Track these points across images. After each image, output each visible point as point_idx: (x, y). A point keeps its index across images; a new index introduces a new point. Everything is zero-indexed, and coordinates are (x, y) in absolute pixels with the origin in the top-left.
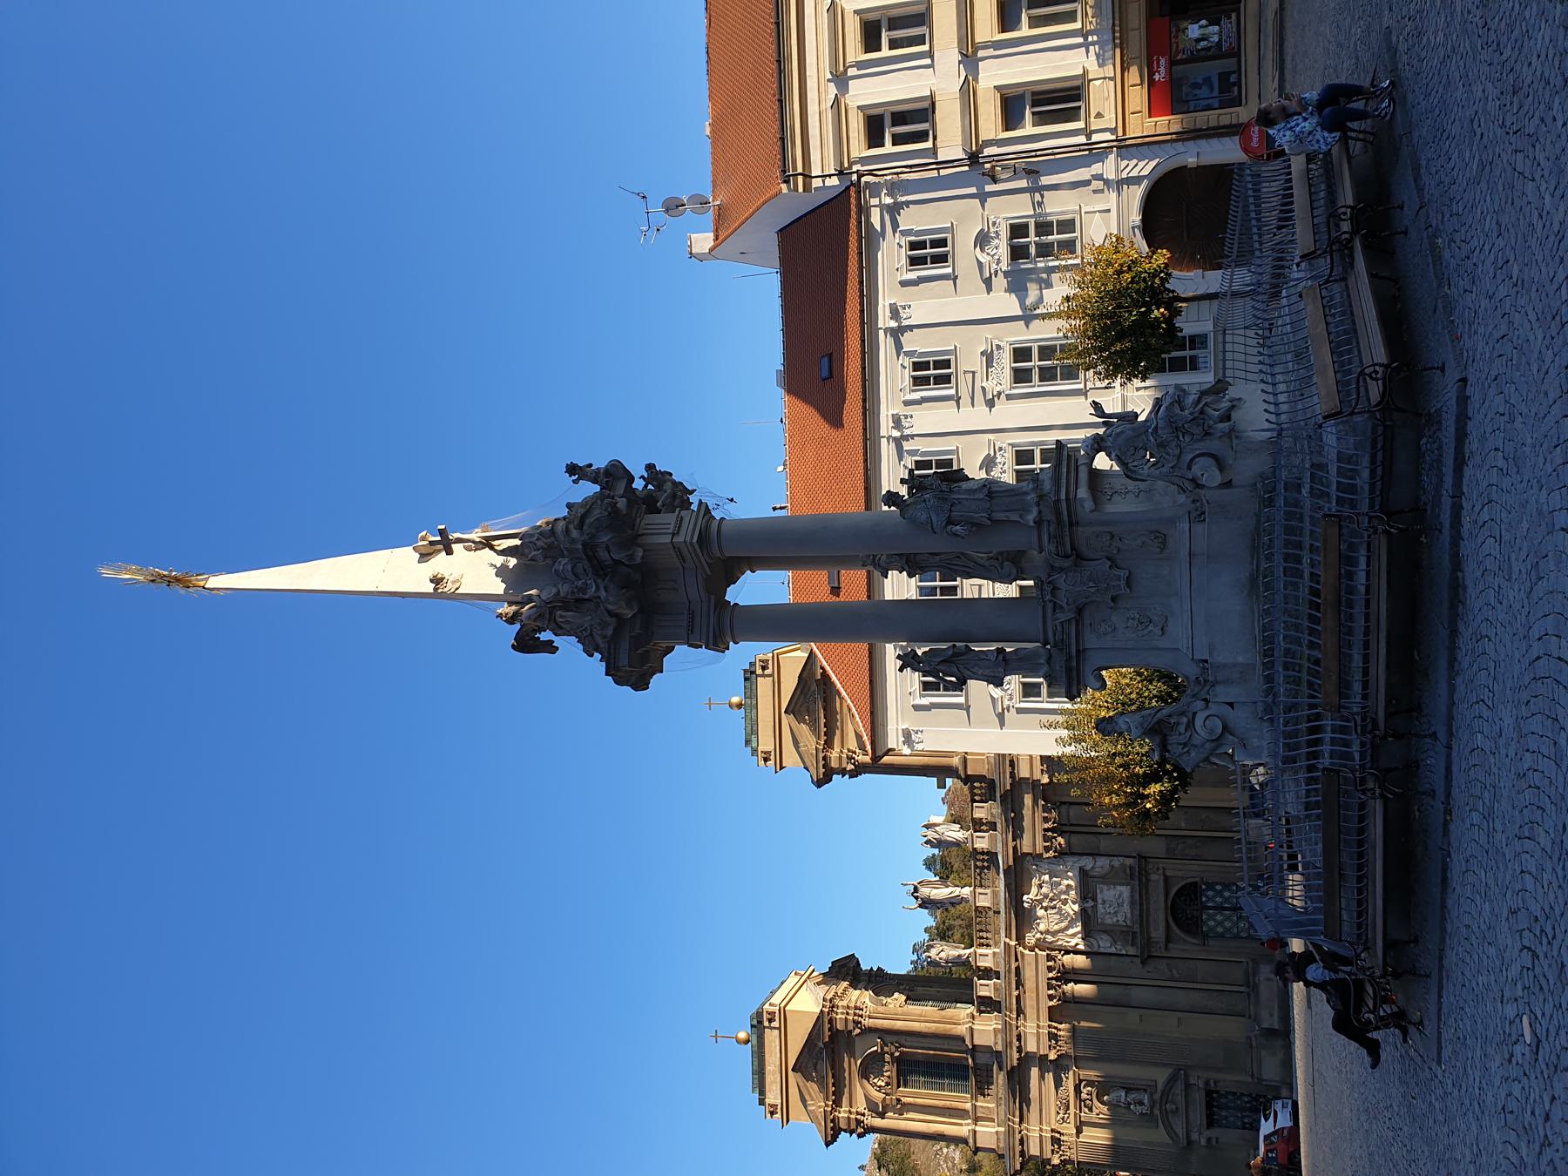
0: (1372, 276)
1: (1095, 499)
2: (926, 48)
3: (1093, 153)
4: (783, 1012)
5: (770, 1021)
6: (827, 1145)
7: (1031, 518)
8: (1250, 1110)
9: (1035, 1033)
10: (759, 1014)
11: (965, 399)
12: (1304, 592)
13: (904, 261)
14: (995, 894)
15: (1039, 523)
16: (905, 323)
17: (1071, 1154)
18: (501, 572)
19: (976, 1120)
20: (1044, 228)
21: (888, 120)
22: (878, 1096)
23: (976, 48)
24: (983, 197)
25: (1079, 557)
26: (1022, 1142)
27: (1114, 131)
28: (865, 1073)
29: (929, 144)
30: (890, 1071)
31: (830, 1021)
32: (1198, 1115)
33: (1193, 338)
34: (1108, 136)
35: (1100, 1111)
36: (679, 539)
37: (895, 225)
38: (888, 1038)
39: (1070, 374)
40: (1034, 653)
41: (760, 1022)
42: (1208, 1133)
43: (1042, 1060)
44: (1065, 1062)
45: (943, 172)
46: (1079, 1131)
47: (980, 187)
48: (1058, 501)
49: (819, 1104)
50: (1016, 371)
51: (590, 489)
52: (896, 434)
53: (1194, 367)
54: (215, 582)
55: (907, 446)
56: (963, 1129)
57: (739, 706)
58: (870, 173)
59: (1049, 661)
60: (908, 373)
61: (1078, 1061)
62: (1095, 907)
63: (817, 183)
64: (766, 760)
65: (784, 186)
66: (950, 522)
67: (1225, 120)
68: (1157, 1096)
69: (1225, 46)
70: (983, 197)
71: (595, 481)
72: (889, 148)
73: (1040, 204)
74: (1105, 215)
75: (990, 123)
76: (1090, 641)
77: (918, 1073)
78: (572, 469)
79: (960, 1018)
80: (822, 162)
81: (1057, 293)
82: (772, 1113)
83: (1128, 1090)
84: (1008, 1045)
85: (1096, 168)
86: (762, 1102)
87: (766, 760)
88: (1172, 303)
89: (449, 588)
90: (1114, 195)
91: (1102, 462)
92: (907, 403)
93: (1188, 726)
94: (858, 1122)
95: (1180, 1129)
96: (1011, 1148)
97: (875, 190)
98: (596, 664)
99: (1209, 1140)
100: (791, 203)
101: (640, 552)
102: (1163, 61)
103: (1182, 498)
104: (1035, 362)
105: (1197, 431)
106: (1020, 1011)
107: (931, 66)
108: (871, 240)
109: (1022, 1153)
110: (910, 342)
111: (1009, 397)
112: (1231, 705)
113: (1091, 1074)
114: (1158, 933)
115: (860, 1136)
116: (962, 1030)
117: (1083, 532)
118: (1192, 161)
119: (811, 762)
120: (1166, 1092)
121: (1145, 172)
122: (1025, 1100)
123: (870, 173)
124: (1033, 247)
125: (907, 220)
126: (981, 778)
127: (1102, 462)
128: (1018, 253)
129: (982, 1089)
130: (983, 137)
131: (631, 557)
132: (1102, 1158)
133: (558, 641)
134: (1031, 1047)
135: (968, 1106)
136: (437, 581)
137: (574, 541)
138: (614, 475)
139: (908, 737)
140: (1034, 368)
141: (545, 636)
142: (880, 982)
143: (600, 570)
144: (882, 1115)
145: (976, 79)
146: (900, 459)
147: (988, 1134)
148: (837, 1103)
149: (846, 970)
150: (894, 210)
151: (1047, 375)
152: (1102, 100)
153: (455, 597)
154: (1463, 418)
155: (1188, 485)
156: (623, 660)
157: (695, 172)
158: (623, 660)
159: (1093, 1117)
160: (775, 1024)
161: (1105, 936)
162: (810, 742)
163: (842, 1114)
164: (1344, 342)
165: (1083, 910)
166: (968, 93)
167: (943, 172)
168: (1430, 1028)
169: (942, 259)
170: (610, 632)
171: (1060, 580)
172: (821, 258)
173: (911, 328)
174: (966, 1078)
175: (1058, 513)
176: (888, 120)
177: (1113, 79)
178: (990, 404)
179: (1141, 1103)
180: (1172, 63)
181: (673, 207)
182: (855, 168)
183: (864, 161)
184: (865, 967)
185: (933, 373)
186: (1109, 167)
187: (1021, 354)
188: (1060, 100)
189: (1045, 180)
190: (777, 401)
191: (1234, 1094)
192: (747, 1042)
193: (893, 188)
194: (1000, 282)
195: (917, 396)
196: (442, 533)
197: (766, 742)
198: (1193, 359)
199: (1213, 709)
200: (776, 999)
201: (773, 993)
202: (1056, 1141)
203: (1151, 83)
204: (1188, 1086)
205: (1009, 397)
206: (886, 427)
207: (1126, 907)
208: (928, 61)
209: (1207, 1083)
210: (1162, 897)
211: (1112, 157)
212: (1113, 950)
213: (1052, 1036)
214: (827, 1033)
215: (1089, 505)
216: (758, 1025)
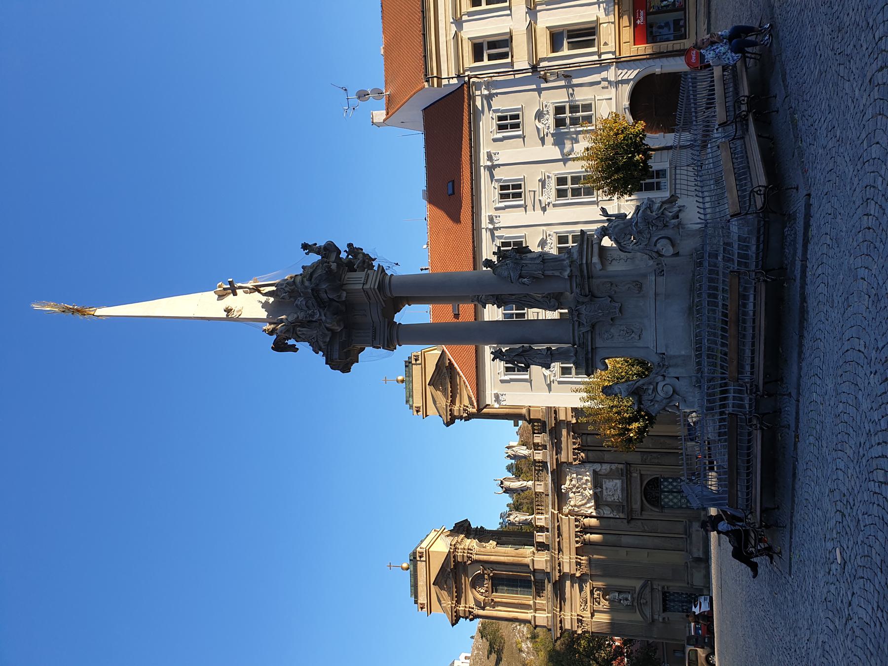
0: (758, 136)
1: (602, 263)
3: (603, 66)
4: (428, 552)
5: (420, 557)
6: (453, 625)
7: (566, 274)
8: (686, 602)
9: (568, 562)
10: (414, 553)
11: (530, 207)
12: (719, 315)
13: (495, 127)
14: (546, 485)
15: (570, 277)
16: (496, 163)
17: (588, 628)
18: (265, 305)
19: (536, 610)
20: (574, 108)
21: (485, 46)
22: (481, 598)
23: (536, 5)
24: (539, 91)
25: (593, 296)
27: (614, 53)
28: (474, 585)
29: (509, 60)
30: (487, 584)
31: (454, 557)
32: (658, 606)
33: (658, 172)
34: (611, 56)
35: (604, 604)
36: (367, 287)
37: (490, 106)
38: (487, 566)
39: (589, 192)
40: (567, 351)
41: (415, 558)
42: (664, 615)
44: (585, 578)
45: (517, 76)
46: (593, 615)
47: (538, 85)
48: (581, 264)
49: (448, 603)
50: (558, 191)
51: (315, 258)
52: (491, 226)
53: (659, 188)
54: (100, 312)
55: (497, 233)
56: (528, 615)
57: (402, 381)
58: (476, 76)
59: (576, 354)
60: (497, 192)
61: (592, 577)
62: (601, 492)
63: (445, 82)
64: (418, 411)
65: (426, 84)
66: (521, 276)
67: (677, 47)
68: (636, 596)
69: (677, 4)
70: (539, 91)
71: (318, 253)
72: (486, 62)
73: (572, 95)
74: (609, 101)
75: (544, 48)
76: (599, 343)
77: (503, 585)
78: (305, 246)
79: (526, 554)
80: (448, 70)
81: (581, 146)
82: (422, 608)
83: (620, 592)
84: (553, 569)
85: (604, 74)
86: (416, 602)
87: (418, 411)
88: (647, 152)
89: (235, 314)
90: (614, 90)
91: (607, 242)
92: (497, 209)
93: (653, 390)
94: (470, 612)
95: (648, 613)
96: (555, 625)
97: (478, 86)
98: (320, 358)
99: (664, 619)
100: (430, 93)
101: (344, 294)
102: (642, 13)
103: (651, 262)
104: (569, 186)
105: (660, 224)
106: (560, 550)
107: (510, 15)
108: (476, 115)
109: (561, 628)
110: (499, 174)
111: (554, 206)
112: (678, 378)
113: (599, 584)
114: (637, 506)
115: (471, 620)
116: (527, 561)
117: (595, 282)
118: (658, 71)
119: (443, 412)
120: (641, 593)
121: (632, 77)
122: (563, 599)
123: (476, 76)
124: (568, 120)
125: (496, 103)
126: (538, 420)
127: (607, 242)
128: (559, 123)
129: (539, 592)
130: (540, 56)
131: (340, 297)
132: (605, 630)
133: (298, 345)
134: (566, 569)
135: (531, 603)
136: (228, 311)
137: (306, 288)
138: (329, 249)
139: (497, 398)
140: (569, 189)
141: (291, 342)
142: (482, 535)
143: (322, 304)
144: (483, 609)
145: (536, 23)
146: (493, 241)
147: (542, 618)
148: (458, 602)
149: (463, 528)
150: (489, 98)
151: (576, 193)
152: (607, 34)
153: (238, 320)
154: (808, 216)
155: (654, 255)
156: (336, 355)
157: (374, 75)
158: (336, 355)
159: (600, 607)
160: (423, 559)
161: (607, 508)
162: (443, 401)
163: (461, 608)
164: (742, 174)
165: (595, 494)
166: (531, 30)
167: (517, 76)
168: (785, 555)
169: (517, 126)
170: (328, 340)
171: (582, 309)
172: (448, 125)
173: (499, 166)
174: (530, 587)
175: (581, 271)
176: (485, 46)
177: (613, 23)
178: (544, 209)
179: (627, 599)
180: (647, 14)
181: (362, 95)
182: (467, 74)
183: (472, 69)
184: (473, 526)
185: (511, 192)
186: (611, 74)
187: (561, 181)
188: (584, 35)
189: (575, 81)
190: (423, 207)
191: (678, 593)
192: (407, 569)
193: (489, 85)
194: (549, 140)
195: (502, 205)
196: (230, 283)
197: (418, 402)
198: (658, 183)
199: (668, 380)
200: (424, 545)
201: (422, 541)
202: (580, 621)
203: (635, 26)
204: (652, 589)
205: (554, 206)
206: (485, 223)
207: (619, 492)
208: (508, 12)
209: (663, 588)
210: (639, 487)
211: (613, 68)
212: (611, 515)
213: (578, 564)
214: (452, 564)
215: (599, 266)
216: (414, 559)
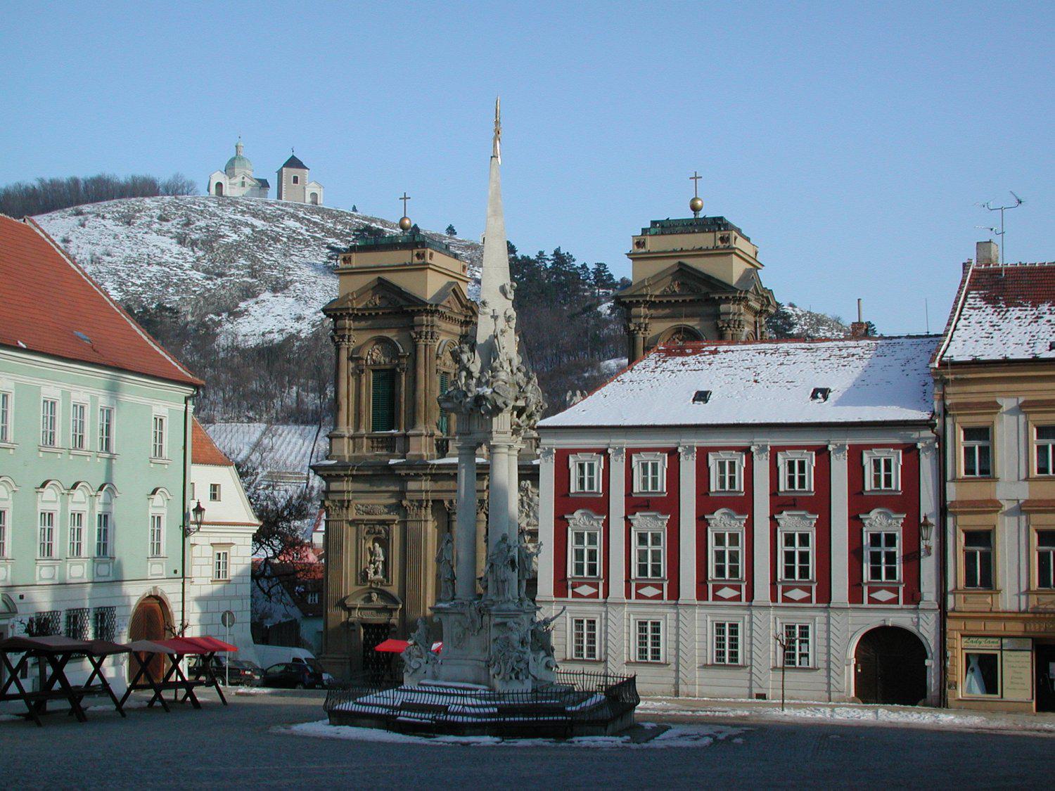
2: (1035, 473)
4: (424, 267)
26: (338, 476)
43: (402, 494)
44: (402, 514)
46: (353, 523)
94: (343, 337)
115: (332, 338)
120: (383, 595)
135: (363, 431)
144: (350, 358)
197: (653, 244)
214: (410, 309)
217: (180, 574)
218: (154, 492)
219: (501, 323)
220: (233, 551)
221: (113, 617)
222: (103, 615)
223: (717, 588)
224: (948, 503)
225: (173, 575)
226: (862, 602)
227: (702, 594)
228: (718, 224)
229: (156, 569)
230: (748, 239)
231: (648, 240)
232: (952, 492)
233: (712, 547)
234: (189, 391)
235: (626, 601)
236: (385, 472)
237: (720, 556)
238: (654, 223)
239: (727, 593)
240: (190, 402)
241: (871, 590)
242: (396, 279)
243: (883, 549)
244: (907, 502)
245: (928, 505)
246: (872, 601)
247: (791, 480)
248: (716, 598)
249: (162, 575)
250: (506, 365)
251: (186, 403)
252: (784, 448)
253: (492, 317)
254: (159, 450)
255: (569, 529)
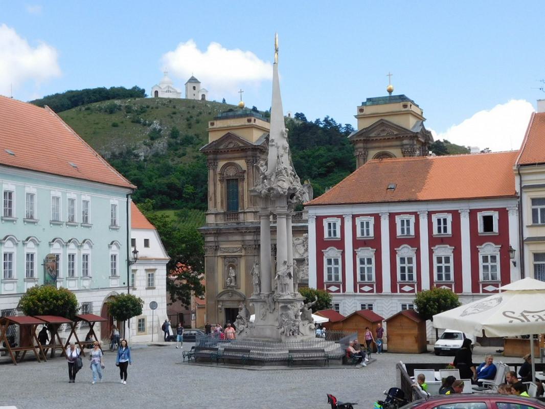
32: (230, 305)
83: (235, 277)
95: (224, 297)
99: (221, 309)
179: (231, 282)
197: (368, 110)
204: (239, 301)
217: (126, 285)
218: (112, 244)
219: (281, 151)
220: (156, 273)
221: (91, 307)
222: (86, 306)
223: (401, 286)
224: (524, 239)
225: (123, 286)
226: (479, 292)
227: (394, 289)
228: (402, 98)
229: (114, 283)
230: (417, 106)
231: (364, 108)
232: (527, 234)
233: (399, 265)
234: (129, 191)
235: (354, 294)
236: (234, 231)
237: (403, 269)
238: (369, 100)
239: (407, 288)
240: (129, 196)
241: (484, 286)
242: (239, 133)
243: (489, 264)
244: (502, 239)
245: (514, 242)
246: (484, 291)
247: (439, 229)
248: (402, 291)
249: (117, 285)
250: (284, 172)
251: (127, 197)
252: (435, 212)
253: (276, 147)
254: (114, 223)
255: (324, 257)
